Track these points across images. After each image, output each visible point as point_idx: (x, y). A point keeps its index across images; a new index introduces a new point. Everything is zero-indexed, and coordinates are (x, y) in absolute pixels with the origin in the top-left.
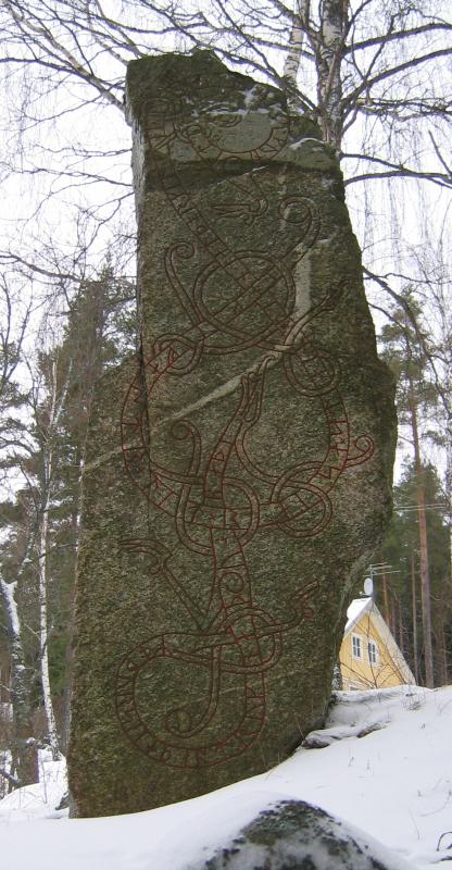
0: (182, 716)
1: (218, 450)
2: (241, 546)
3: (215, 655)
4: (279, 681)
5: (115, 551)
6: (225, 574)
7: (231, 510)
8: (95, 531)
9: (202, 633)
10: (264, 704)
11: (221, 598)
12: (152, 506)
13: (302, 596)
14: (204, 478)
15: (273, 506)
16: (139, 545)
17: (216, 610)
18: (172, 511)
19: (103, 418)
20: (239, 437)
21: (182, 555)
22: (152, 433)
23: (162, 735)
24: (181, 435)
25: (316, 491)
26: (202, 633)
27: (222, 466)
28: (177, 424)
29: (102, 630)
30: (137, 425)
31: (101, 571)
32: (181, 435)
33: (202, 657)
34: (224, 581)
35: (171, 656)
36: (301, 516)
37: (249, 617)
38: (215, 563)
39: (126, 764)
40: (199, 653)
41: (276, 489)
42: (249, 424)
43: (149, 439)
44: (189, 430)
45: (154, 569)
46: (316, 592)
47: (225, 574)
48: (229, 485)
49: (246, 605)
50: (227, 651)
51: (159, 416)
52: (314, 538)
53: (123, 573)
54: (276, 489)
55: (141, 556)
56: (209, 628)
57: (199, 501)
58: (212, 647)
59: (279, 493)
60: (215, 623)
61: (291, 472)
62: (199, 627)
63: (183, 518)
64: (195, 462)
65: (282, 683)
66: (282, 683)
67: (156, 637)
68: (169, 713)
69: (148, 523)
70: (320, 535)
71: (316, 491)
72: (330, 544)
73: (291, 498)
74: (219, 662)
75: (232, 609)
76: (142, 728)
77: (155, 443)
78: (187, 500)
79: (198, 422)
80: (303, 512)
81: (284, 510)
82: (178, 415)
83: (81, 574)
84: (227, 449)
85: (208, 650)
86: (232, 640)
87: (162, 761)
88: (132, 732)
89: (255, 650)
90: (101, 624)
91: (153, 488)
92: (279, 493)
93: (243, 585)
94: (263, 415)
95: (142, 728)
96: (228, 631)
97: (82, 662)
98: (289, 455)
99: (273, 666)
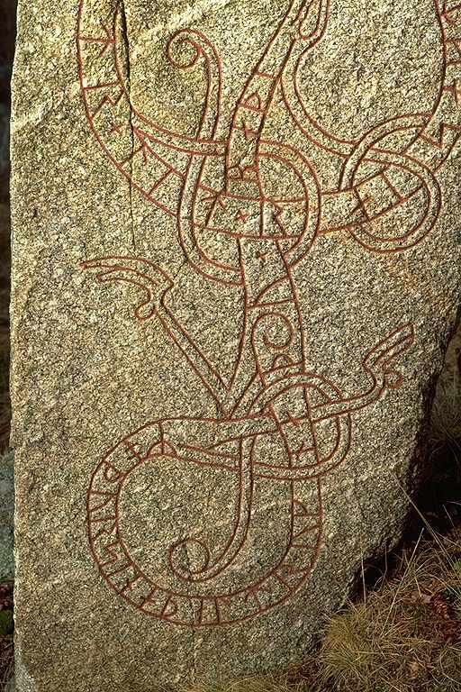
0: (193, 549)
1: (250, 90)
2: (287, 267)
3: (245, 452)
4: (343, 490)
5: (78, 280)
6: (262, 316)
7: (273, 203)
8: (40, 243)
9: (223, 416)
10: (319, 525)
11: (255, 357)
12: (135, 192)
13: (384, 353)
14: (225, 141)
15: (343, 196)
16: (116, 267)
17: (246, 377)
18: (172, 205)
19: (44, 26)
20: (289, 67)
21: (190, 283)
22: (134, 56)
23: (164, 581)
24: (186, 58)
25: (418, 168)
26: (223, 416)
27: (258, 121)
28: (176, 38)
29: (62, 418)
30: (107, 42)
31: (54, 317)
32: (186, 58)
33: (225, 455)
34: (260, 328)
35: (174, 454)
36: (390, 214)
37: (299, 390)
38: (244, 297)
39: (107, 623)
40: (218, 449)
41: (349, 166)
42: (305, 43)
43: (128, 67)
44: (197, 48)
45: (146, 308)
46: (408, 344)
47: (262, 316)
48: (268, 155)
49: (294, 369)
50: (264, 444)
51: (147, 22)
52: (407, 254)
53: (93, 319)
54: (349, 166)
55: (122, 287)
56: (236, 406)
57: (218, 190)
58: (241, 438)
59: (353, 173)
60: (246, 399)
61: (376, 133)
62: (219, 407)
63: (190, 218)
64: (209, 114)
65: (350, 492)
66: (350, 492)
67: (149, 424)
68: (173, 547)
69: (131, 228)
70: (420, 248)
71: (418, 168)
72: (434, 264)
73: (374, 181)
74: (250, 463)
75: (272, 376)
76: (131, 570)
77: (138, 75)
78: (197, 185)
79: (215, 33)
80: (391, 207)
81: (360, 204)
82: (177, 20)
83: (22, 322)
84: (267, 87)
85: (234, 444)
86: (272, 426)
87: (163, 616)
88: (114, 579)
89: (309, 444)
90: (57, 407)
91: (137, 159)
92: (353, 173)
93: (291, 335)
94: (332, 24)
95: (131, 570)
96: (266, 411)
97: (32, 472)
98: (373, 102)
99: (335, 466)
